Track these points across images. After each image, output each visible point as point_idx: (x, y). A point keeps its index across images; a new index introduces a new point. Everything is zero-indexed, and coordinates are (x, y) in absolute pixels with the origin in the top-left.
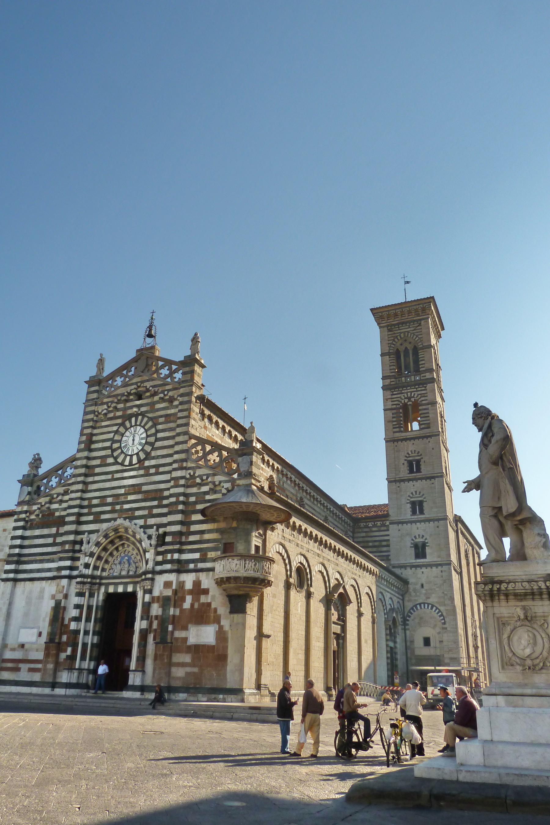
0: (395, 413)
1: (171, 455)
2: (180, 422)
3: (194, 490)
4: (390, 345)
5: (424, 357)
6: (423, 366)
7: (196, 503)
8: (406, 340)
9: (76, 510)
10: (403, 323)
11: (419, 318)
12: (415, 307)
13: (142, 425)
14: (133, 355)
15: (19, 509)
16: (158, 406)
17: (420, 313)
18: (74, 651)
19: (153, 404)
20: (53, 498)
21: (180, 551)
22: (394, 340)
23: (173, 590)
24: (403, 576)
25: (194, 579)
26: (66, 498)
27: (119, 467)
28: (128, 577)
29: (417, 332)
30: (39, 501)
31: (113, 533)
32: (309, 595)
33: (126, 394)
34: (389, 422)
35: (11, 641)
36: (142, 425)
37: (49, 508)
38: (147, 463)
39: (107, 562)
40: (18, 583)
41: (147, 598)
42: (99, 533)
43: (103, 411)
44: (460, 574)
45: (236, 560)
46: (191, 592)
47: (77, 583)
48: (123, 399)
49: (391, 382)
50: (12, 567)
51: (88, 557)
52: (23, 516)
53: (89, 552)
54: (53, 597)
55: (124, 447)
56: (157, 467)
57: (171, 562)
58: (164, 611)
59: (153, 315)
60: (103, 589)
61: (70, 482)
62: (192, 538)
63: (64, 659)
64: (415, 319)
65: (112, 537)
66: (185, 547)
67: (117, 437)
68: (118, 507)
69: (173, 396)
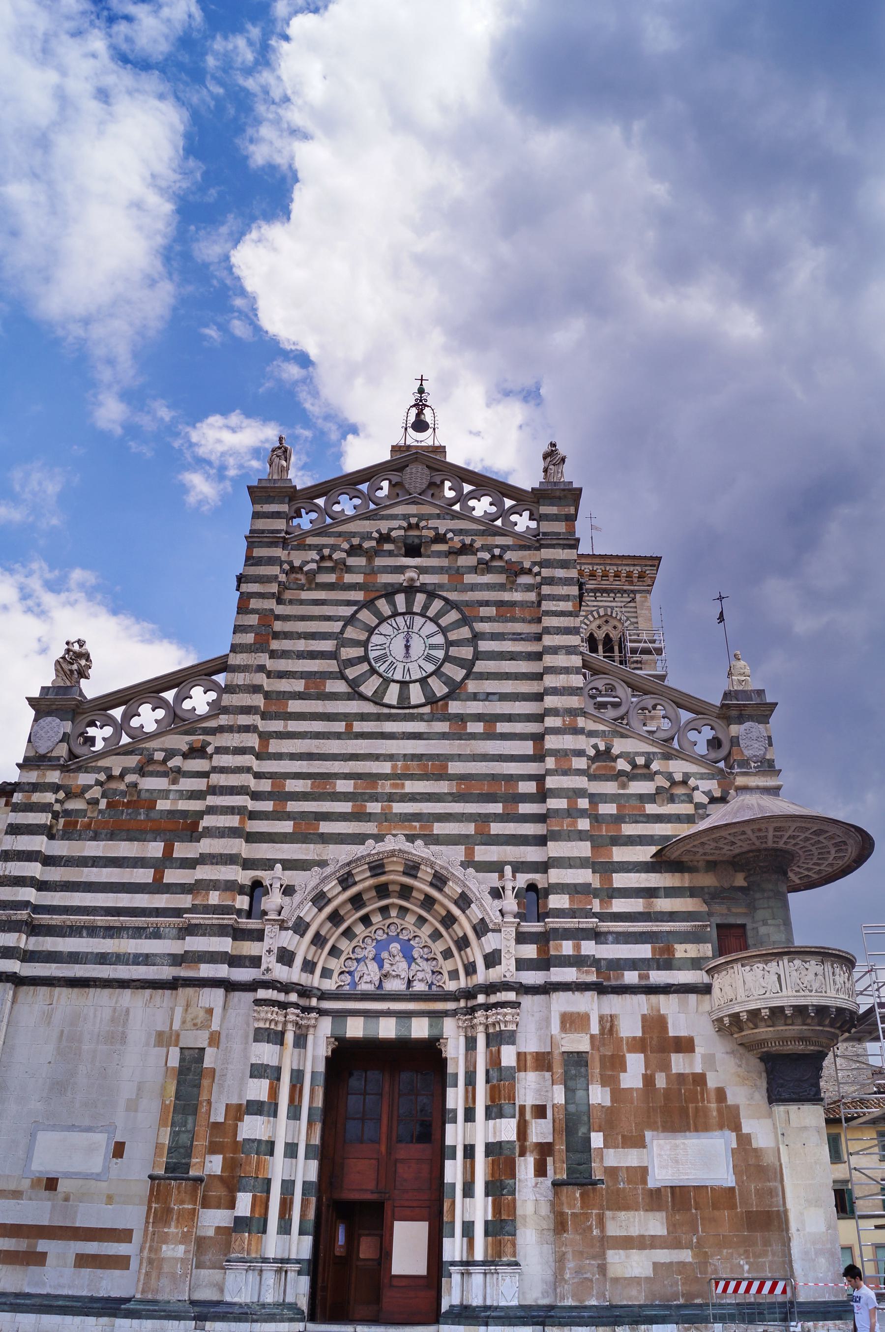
7: (619, 819)
8: (607, 622)
10: (603, 591)
15: (33, 777)
17: (635, 580)
18: (261, 1204)
20: (150, 760)
21: (597, 936)
29: (629, 612)
30: (101, 763)
31: (368, 874)
37: (135, 785)
38: (455, 707)
40: (24, 989)
42: (328, 870)
47: (258, 1002)
51: (290, 932)
52: (49, 797)
53: (294, 919)
56: (490, 719)
57: (578, 961)
62: (619, 905)
63: (218, 1229)
64: (625, 588)
65: (367, 883)
68: (374, 807)
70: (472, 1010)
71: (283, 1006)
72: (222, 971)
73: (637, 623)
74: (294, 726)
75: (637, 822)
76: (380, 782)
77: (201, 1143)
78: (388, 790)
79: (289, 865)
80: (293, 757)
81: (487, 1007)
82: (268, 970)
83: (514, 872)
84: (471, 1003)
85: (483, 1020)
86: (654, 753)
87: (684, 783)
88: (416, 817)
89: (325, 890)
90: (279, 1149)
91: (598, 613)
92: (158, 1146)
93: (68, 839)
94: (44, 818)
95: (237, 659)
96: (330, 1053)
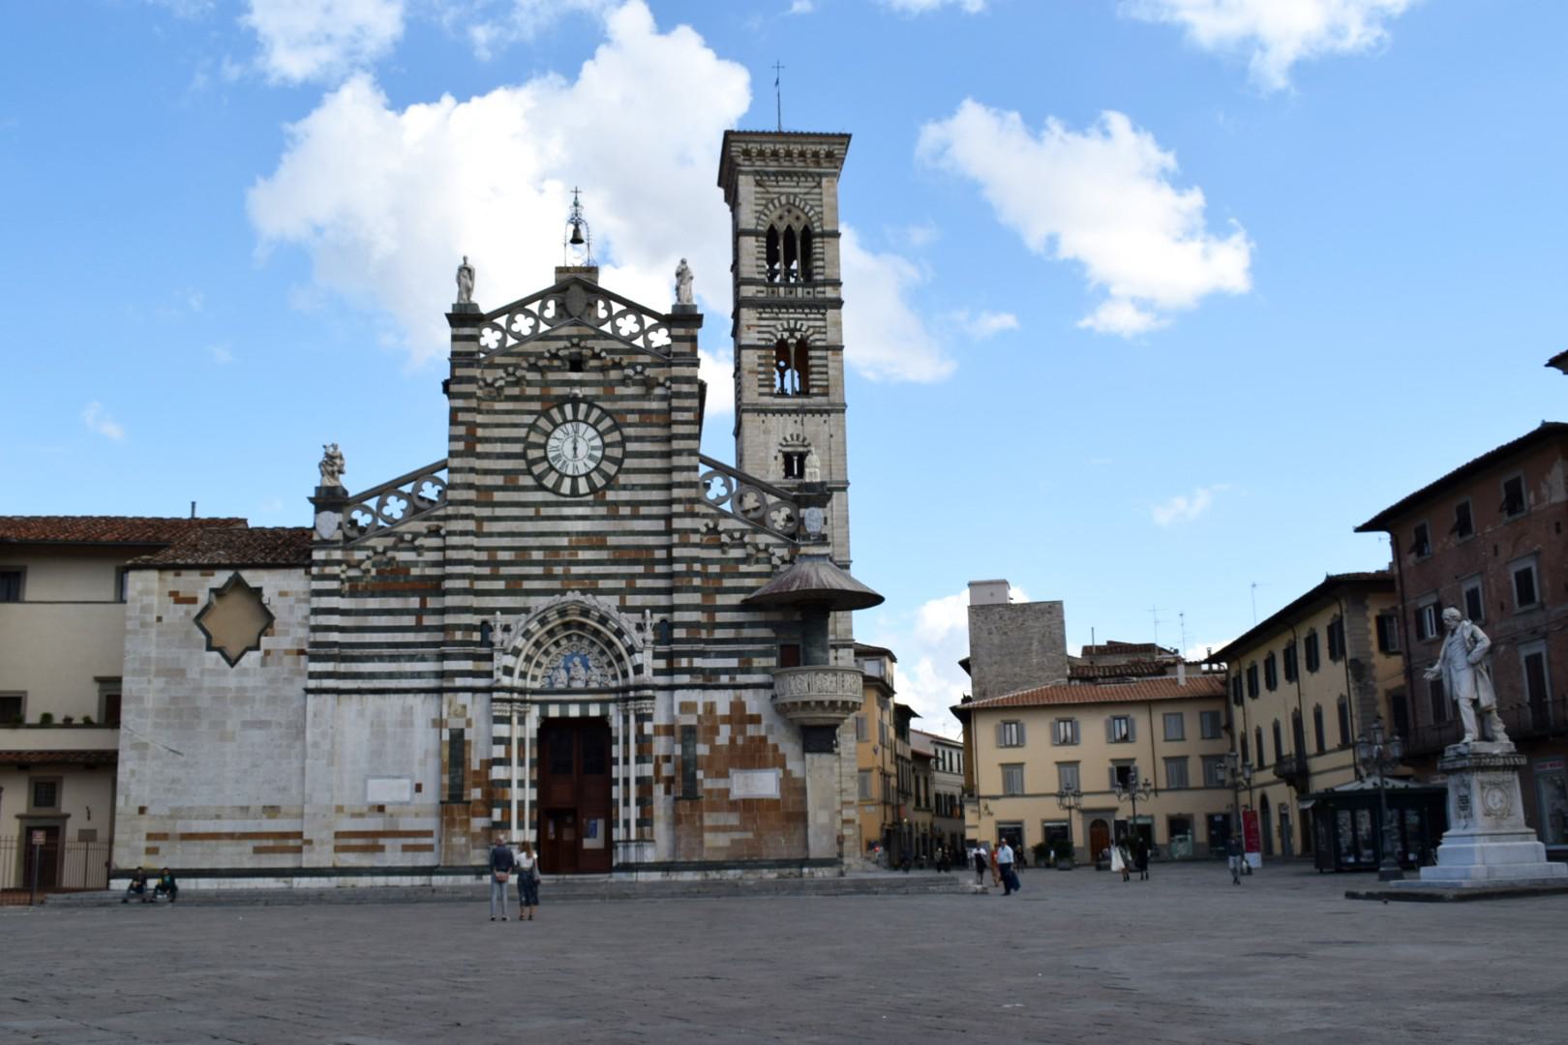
0: (765, 357)
4: (758, 215)
5: (823, 253)
6: (821, 270)
7: (720, 576)
11: (818, 170)
12: (814, 148)
13: (591, 420)
14: (549, 281)
16: (620, 390)
17: (822, 161)
18: (507, 813)
19: (610, 385)
20: (402, 540)
21: (703, 654)
22: (766, 206)
23: (699, 717)
25: (732, 699)
27: (551, 497)
29: (813, 200)
30: (369, 543)
33: (547, 355)
34: (751, 372)
36: (591, 420)
37: (393, 558)
38: (611, 496)
42: (531, 615)
43: (496, 380)
45: (830, 675)
46: (727, 720)
47: (494, 700)
48: (541, 363)
49: (758, 292)
50: (329, 667)
51: (510, 656)
52: (336, 570)
54: (439, 723)
55: (554, 458)
56: (634, 504)
58: (684, 748)
59: (576, 198)
61: (441, 512)
62: (719, 634)
63: (483, 829)
64: (810, 170)
66: (709, 648)
67: (534, 438)
68: (558, 570)
69: (657, 379)
70: (626, 700)
71: (510, 701)
72: (469, 682)
73: (821, 213)
74: (499, 512)
75: (733, 577)
76: (562, 552)
77: (468, 782)
78: (567, 558)
79: (505, 611)
80: (501, 535)
81: (636, 699)
82: (498, 680)
83: (652, 613)
84: (625, 695)
85: (633, 707)
86: (747, 530)
87: (766, 550)
88: (587, 576)
89: (530, 627)
90: (515, 784)
91: (780, 201)
92: (442, 786)
93: (354, 597)
94: (334, 585)
95: (456, 463)
96: (539, 726)
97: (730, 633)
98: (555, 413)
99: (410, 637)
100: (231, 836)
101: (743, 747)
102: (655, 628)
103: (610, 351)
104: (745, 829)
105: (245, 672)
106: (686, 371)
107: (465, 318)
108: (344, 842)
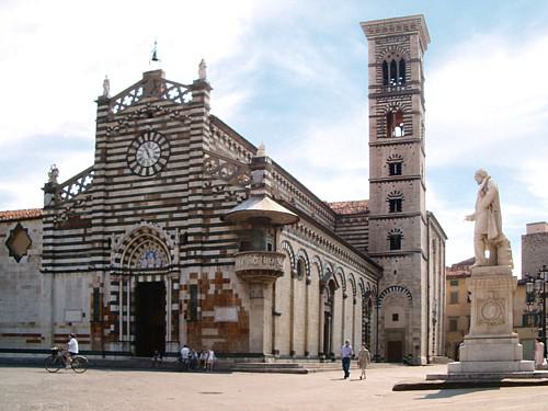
1: (187, 168)
2: (193, 139)
3: (211, 198)
7: (213, 209)
9: (100, 214)
14: (141, 78)
16: (169, 124)
18: (117, 327)
19: (165, 122)
21: (202, 249)
24: (380, 264)
26: (89, 203)
27: (138, 178)
28: (154, 269)
32: (308, 282)
35: (59, 321)
38: (163, 174)
39: (134, 257)
41: (176, 286)
44: (428, 260)
46: (213, 282)
50: (50, 261)
52: (51, 219)
57: (195, 257)
60: (133, 279)
62: (211, 238)
66: (206, 245)
67: (132, 151)
68: (140, 212)
72: (100, 266)
74: (116, 187)
88: (152, 214)
94: (50, 225)
95: (97, 166)
97: (216, 238)
98: (140, 138)
99: (80, 247)
100: (18, 335)
101: (221, 296)
102: (181, 237)
103: (164, 107)
104: (221, 337)
105: (22, 265)
106: (199, 110)
107: (104, 102)
108: (57, 339)
